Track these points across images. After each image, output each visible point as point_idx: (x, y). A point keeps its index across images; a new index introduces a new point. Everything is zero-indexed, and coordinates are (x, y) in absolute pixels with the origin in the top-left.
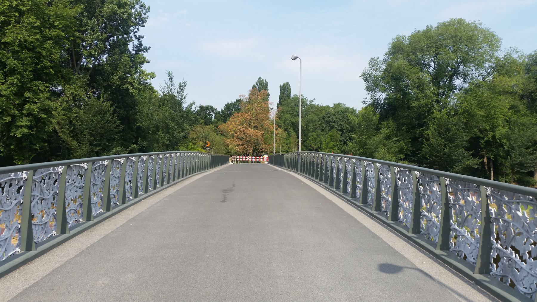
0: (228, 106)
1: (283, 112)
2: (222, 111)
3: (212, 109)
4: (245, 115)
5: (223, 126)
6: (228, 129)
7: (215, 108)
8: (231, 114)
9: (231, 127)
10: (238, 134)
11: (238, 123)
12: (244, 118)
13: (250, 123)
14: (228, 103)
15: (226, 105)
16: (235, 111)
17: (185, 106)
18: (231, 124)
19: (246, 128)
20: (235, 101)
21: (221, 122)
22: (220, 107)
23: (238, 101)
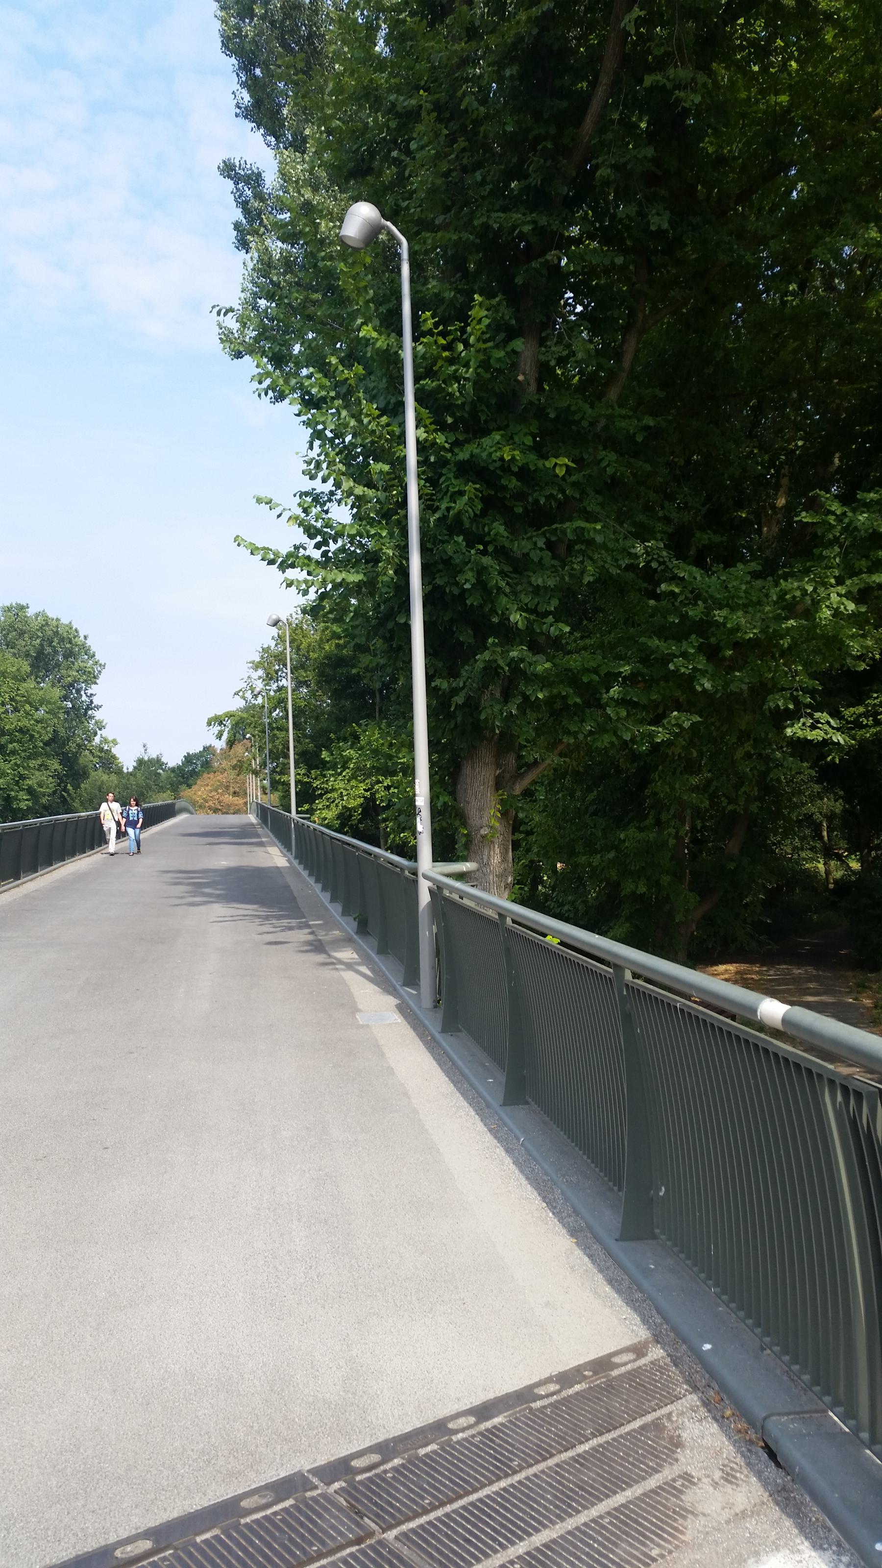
6: (194, 797)
8: (194, 774)
9: (200, 793)
10: (210, 803)
11: (209, 788)
12: (219, 781)
13: (227, 787)
16: (202, 767)
17: (125, 770)
19: (222, 794)
21: (184, 787)
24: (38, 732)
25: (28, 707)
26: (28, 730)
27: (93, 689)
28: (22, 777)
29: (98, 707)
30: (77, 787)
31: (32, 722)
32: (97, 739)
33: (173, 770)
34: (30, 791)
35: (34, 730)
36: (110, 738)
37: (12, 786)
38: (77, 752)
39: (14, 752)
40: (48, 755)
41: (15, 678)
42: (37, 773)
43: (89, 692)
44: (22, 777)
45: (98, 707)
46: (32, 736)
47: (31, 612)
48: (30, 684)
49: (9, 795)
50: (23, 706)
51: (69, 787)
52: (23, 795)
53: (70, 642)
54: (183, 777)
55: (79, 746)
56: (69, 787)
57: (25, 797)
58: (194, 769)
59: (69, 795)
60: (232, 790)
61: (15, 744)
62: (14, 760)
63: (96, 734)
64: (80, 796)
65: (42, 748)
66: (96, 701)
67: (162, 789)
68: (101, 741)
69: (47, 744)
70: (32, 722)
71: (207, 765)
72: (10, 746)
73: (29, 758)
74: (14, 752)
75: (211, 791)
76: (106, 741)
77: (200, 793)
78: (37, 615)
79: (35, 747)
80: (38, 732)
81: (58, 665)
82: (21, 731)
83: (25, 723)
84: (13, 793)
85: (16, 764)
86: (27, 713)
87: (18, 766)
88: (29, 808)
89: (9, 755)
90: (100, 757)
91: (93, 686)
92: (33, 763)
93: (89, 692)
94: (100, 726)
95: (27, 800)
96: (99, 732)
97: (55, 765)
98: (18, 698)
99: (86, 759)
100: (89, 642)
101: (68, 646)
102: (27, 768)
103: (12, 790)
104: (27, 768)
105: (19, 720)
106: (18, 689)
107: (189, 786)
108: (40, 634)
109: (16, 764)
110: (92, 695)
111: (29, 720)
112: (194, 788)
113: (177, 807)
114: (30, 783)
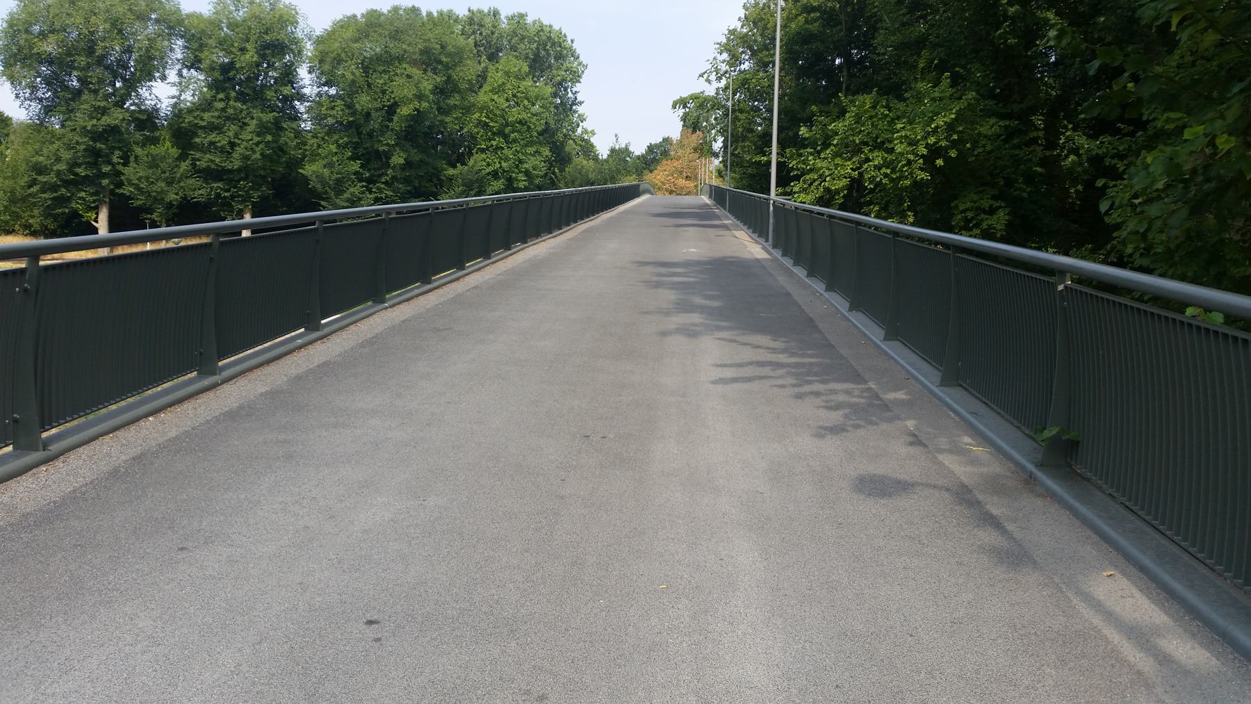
0: (651, 148)
2: (643, 156)
6: (654, 180)
9: (659, 177)
13: (681, 172)
14: (651, 144)
16: (661, 155)
18: (659, 175)
19: (677, 178)
20: (661, 140)
21: (646, 172)
22: (639, 149)
23: (666, 140)
24: (534, 124)
25: (526, 102)
26: (526, 122)
27: (578, 87)
28: (521, 162)
29: (581, 103)
30: (562, 170)
31: (529, 115)
32: (579, 130)
33: (638, 157)
34: (527, 173)
36: (590, 130)
37: (513, 169)
38: (563, 141)
39: (515, 141)
40: (540, 144)
41: (517, 77)
42: (532, 158)
43: (574, 89)
44: (521, 162)
45: (581, 103)
46: (529, 127)
47: (529, 20)
48: (528, 83)
49: (511, 176)
50: (522, 101)
51: (556, 170)
52: (521, 177)
53: (560, 47)
54: (646, 164)
55: (565, 135)
56: (556, 170)
57: (523, 178)
58: (655, 157)
59: (556, 177)
60: (685, 175)
61: (516, 134)
62: (516, 147)
63: (578, 126)
64: (565, 178)
65: (537, 138)
66: (580, 98)
67: (629, 173)
69: (541, 134)
70: (529, 115)
71: (665, 153)
72: (512, 135)
74: (515, 141)
75: (668, 176)
76: (585, 131)
77: (659, 177)
78: (534, 22)
79: (531, 136)
80: (534, 124)
81: (550, 66)
82: (520, 122)
83: (524, 116)
84: (514, 175)
85: (516, 150)
86: (525, 107)
87: (518, 152)
89: (511, 143)
90: (581, 146)
91: (577, 84)
92: (530, 150)
93: (574, 89)
95: (524, 181)
97: (546, 152)
98: (518, 94)
99: (570, 147)
100: (575, 46)
101: (558, 49)
102: (525, 154)
103: (513, 172)
104: (525, 154)
105: (519, 114)
106: (519, 87)
107: (651, 171)
108: (536, 39)
109: (516, 150)
110: (576, 92)
111: (527, 113)
113: (641, 188)
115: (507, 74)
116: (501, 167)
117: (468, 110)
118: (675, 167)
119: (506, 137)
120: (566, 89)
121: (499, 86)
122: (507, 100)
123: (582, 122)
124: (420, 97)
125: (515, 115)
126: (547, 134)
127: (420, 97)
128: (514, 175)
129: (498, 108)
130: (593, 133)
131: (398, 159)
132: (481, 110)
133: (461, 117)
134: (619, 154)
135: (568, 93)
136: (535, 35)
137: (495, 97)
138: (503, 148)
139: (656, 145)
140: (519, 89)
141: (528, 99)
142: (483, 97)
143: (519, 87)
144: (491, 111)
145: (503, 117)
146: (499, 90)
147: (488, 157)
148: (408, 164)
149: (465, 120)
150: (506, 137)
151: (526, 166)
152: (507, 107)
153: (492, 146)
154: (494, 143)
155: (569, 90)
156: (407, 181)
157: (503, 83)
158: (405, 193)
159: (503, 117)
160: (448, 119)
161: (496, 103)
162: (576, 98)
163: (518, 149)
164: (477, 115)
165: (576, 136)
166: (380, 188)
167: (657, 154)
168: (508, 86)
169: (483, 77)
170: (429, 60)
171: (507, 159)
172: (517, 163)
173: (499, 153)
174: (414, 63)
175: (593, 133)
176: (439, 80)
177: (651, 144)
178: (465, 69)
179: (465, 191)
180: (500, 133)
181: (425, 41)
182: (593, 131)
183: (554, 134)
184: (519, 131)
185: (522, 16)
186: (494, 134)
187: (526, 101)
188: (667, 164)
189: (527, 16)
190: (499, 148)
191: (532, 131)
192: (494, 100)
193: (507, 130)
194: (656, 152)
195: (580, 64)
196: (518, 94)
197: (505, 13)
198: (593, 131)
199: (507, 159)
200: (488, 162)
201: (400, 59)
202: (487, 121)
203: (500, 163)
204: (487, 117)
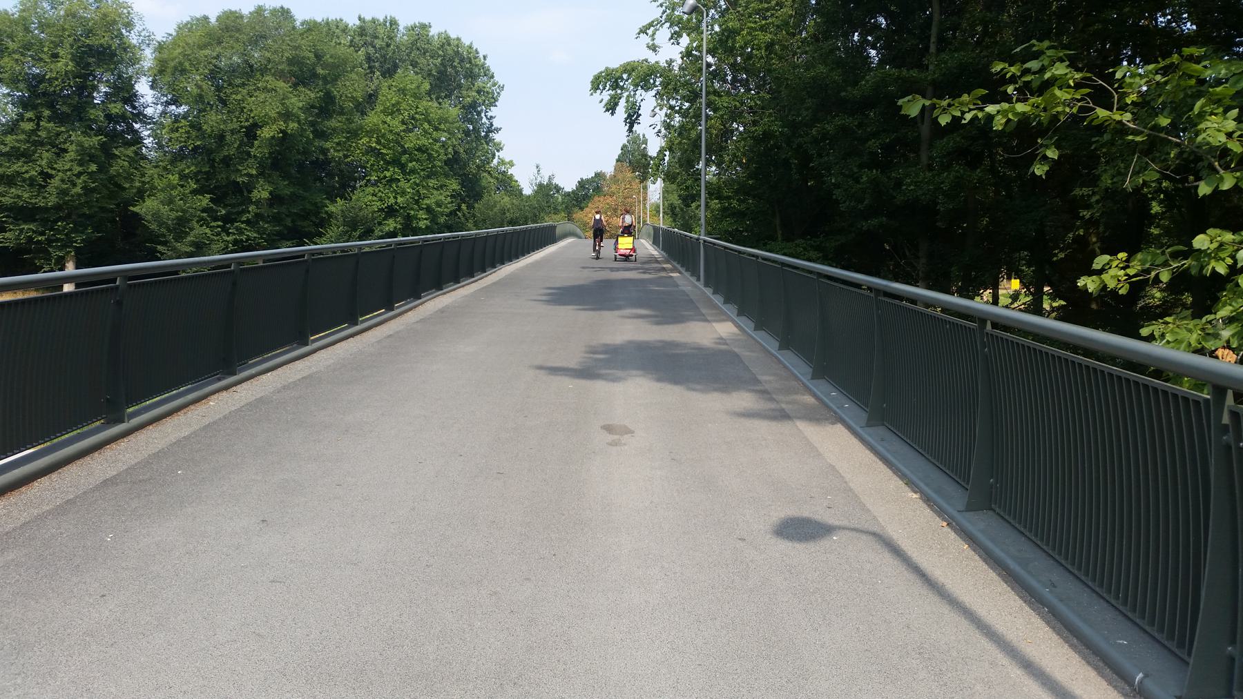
0: (582, 184)
1: (667, 191)
2: (573, 192)
3: (558, 189)
4: (609, 200)
5: (578, 215)
6: (586, 219)
7: (562, 187)
8: (587, 198)
14: (582, 179)
15: (579, 182)
16: (593, 191)
19: (611, 217)
20: (593, 175)
21: (576, 209)
22: (569, 185)
23: (598, 175)
25: (426, 126)
27: (493, 111)
29: (498, 130)
31: (431, 141)
32: (495, 161)
33: (568, 194)
34: (429, 210)
35: (433, 150)
36: (507, 160)
37: (411, 205)
39: (413, 171)
40: (447, 176)
41: (415, 96)
42: (435, 192)
43: (489, 114)
45: (498, 130)
46: (430, 155)
47: (433, 32)
49: (409, 214)
53: (470, 62)
54: (577, 201)
55: (478, 167)
57: (423, 216)
61: (414, 163)
62: (414, 179)
64: (474, 216)
65: (441, 167)
66: (496, 124)
67: (556, 211)
68: (499, 162)
69: (447, 162)
70: (431, 141)
71: (598, 190)
72: (410, 165)
73: (429, 177)
74: (413, 171)
76: (502, 162)
78: (439, 34)
80: (437, 151)
81: (460, 86)
82: (419, 149)
83: (424, 141)
84: (412, 212)
85: (415, 182)
88: (427, 227)
90: (497, 179)
93: (489, 114)
94: (499, 148)
95: (426, 219)
96: (497, 154)
97: (454, 185)
98: (417, 116)
99: (486, 180)
100: (488, 63)
101: (468, 66)
102: (427, 187)
103: (412, 209)
104: (427, 187)
105: (418, 139)
106: (417, 107)
107: (582, 209)
108: (441, 53)
110: (491, 117)
111: (428, 139)
112: (586, 210)
114: (428, 202)
115: (403, 91)
116: (396, 203)
117: (354, 134)
118: (608, 204)
119: (402, 167)
120: (479, 114)
121: (393, 105)
122: (403, 122)
123: (498, 151)
124: (287, 116)
125: (411, 141)
126: (454, 164)
127: (287, 116)
128: (412, 212)
129: (391, 131)
130: (511, 164)
131: (262, 192)
132: (369, 133)
133: (345, 143)
134: (546, 191)
135: (482, 118)
136: (439, 49)
137: (388, 119)
138: (399, 180)
139: (587, 180)
140: (418, 110)
141: (429, 123)
142: (373, 119)
143: (417, 107)
144: (383, 136)
145: (398, 143)
146: (393, 111)
147: (380, 191)
148: (275, 199)
149: (351, 146)
150: (402, 167)
151: (427, 201)
152: (404, 131)
153: (385, 177)
154: (388, 174)
155: (483, 115)
156: (276, 219)
157: (398, 103)
158: (274, 234)
159: (398, 143)
160: (328, 145)
161: (389, 126)
162: (492, 125)
163: (418, 182)
164: (365, 140)
165: (491, 167)
166: (241, 228)
167: (588, 190)
168: (404, 106)
169: (371, 98)
170: (301, 75)
171: (403, 193)
172: (416, 198)
173: (394, 185)
174: (280, 75)
175: (511, 164)
176: (313, 95)
177: (582, 179)
178: (348, 83)
179: (347, 232)
180: (396, 162)
181: (296, 48)
182: (511, 161)
183: (465, 165)
184: (418, 161)
185: (424, 27)
186: (388, 163)
187: (426, 124)
188: (599, 201)
189: (430, 27)
190: (392, 180)
191: (434, 160)
192: (385, 123)
193: (404, 158)
194: (587, 188)
195: (494, 85)
196: (417, 116)
197: (404, 22)
198: (511, 161)
199: (403, 193)
200: (381, 197)
201: (264, 71)
202: (378, 147)
203: (395, 198)
204: (378, 142)
